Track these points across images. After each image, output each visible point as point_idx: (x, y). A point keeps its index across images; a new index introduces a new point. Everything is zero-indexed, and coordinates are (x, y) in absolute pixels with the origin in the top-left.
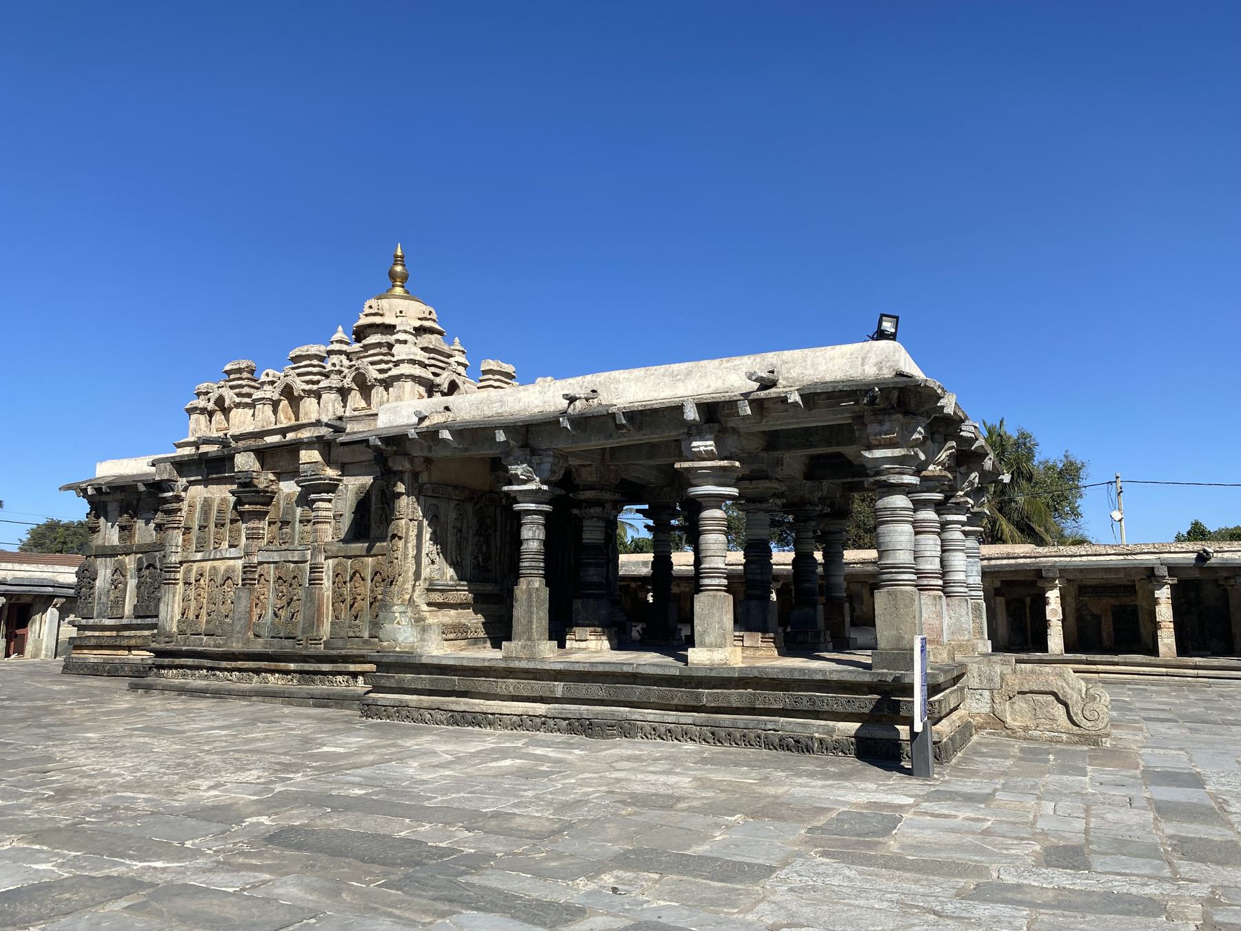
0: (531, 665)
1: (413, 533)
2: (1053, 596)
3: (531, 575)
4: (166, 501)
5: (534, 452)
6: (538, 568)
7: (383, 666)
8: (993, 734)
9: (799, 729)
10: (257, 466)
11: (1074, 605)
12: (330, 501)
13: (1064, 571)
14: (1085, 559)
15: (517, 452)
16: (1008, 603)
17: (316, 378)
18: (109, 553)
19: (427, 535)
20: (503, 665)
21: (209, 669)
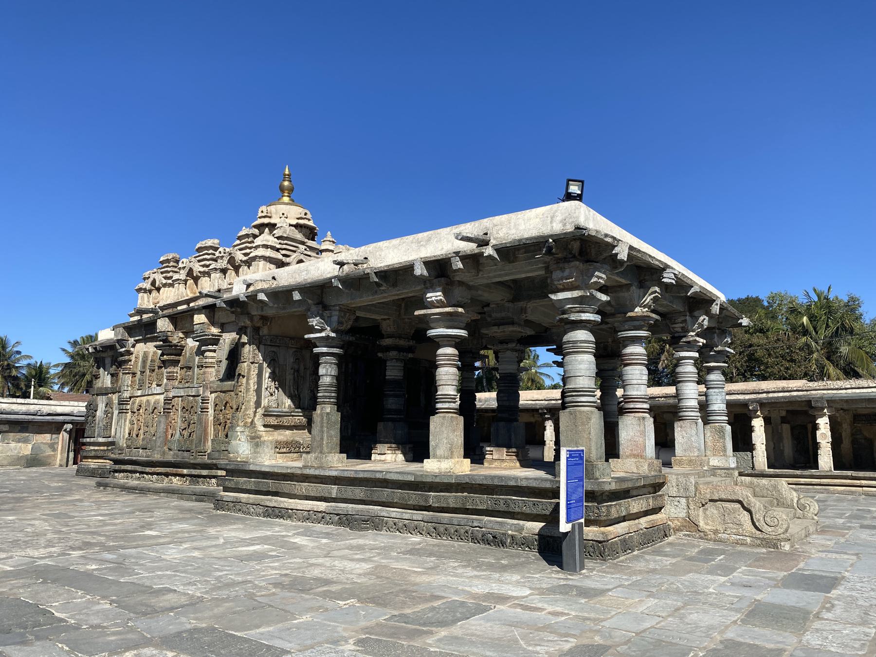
0: (317, 472)
1: (254, 373)
2: (823, 423)
3: (324, 403)
4: (122, 355)
5: (325, 307)
6: (330, 397)
7: (232, 472)
8: (689, 536)
9: (497, 527)
10: (171, 328)
11: (849, 430)
12: (214, 351)
13: (831, 402)
14: (849, 391)
15: (314, 308)
16: (792, 429)
17: (208, 263)
18: (104, 392)
19: (267, 372)
20: (299, 472)
21: (141, 473)
